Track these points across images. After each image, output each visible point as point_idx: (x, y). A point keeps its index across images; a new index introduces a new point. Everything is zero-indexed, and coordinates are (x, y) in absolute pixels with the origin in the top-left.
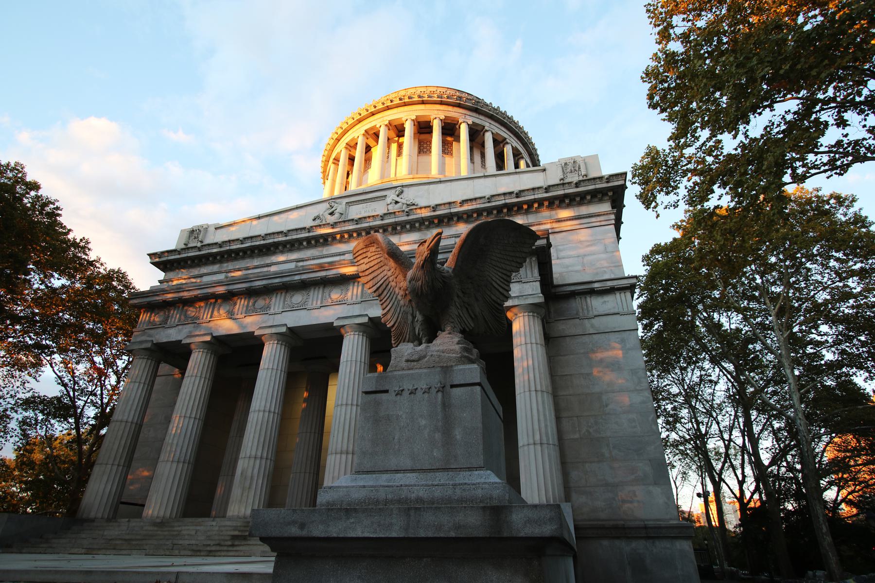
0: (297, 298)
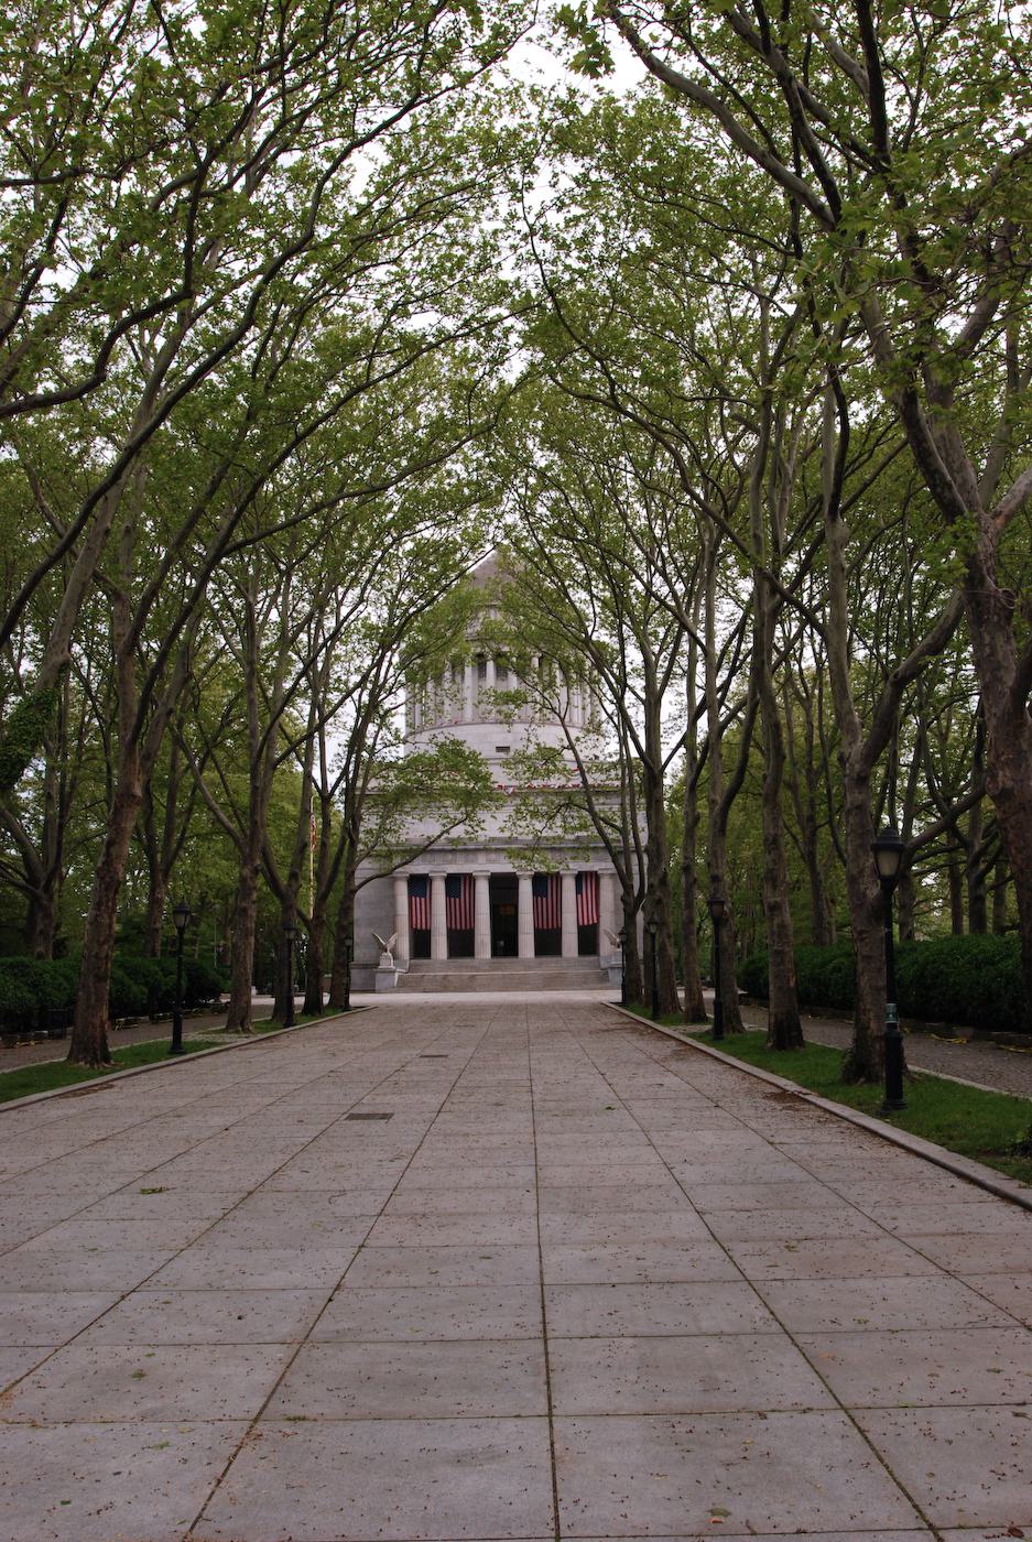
0: (493, 856)
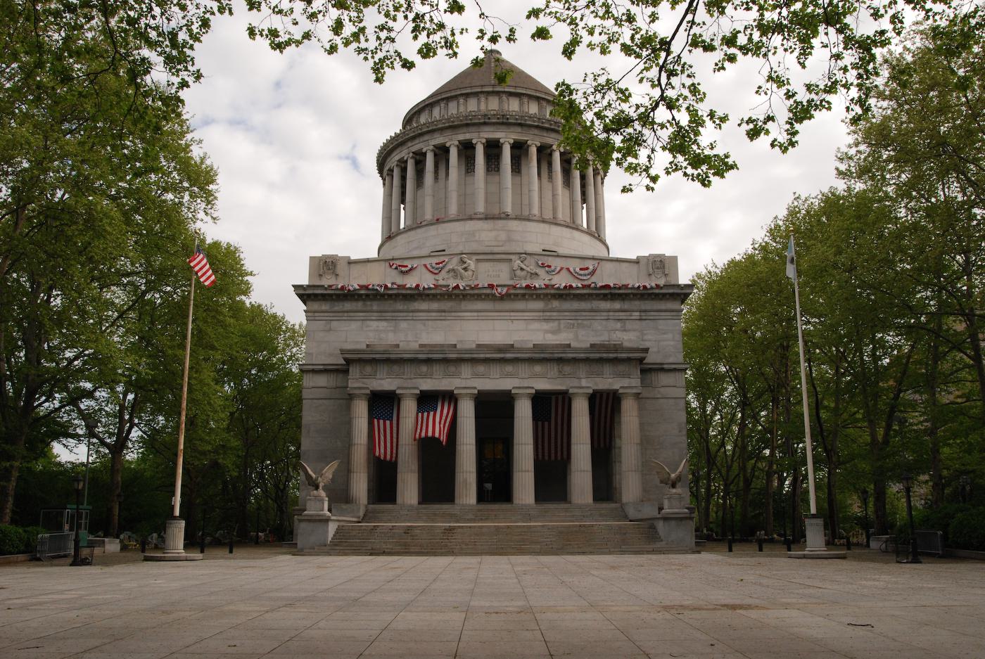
0: (481, 368)
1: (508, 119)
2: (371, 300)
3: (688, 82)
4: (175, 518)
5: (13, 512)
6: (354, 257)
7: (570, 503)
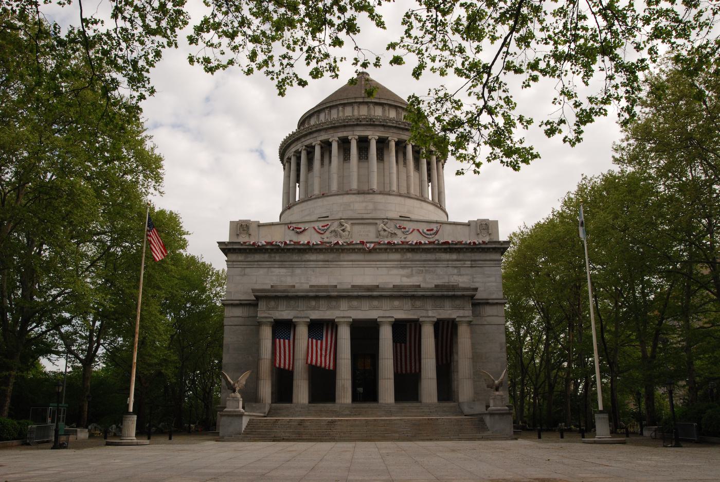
0: (355, 303)
1: (374, 121)
2: (275, 253)
3: (504, 95)
4: (130, 413)
5: (10, 409)
6: (261, 222)
7: (421, 402)
